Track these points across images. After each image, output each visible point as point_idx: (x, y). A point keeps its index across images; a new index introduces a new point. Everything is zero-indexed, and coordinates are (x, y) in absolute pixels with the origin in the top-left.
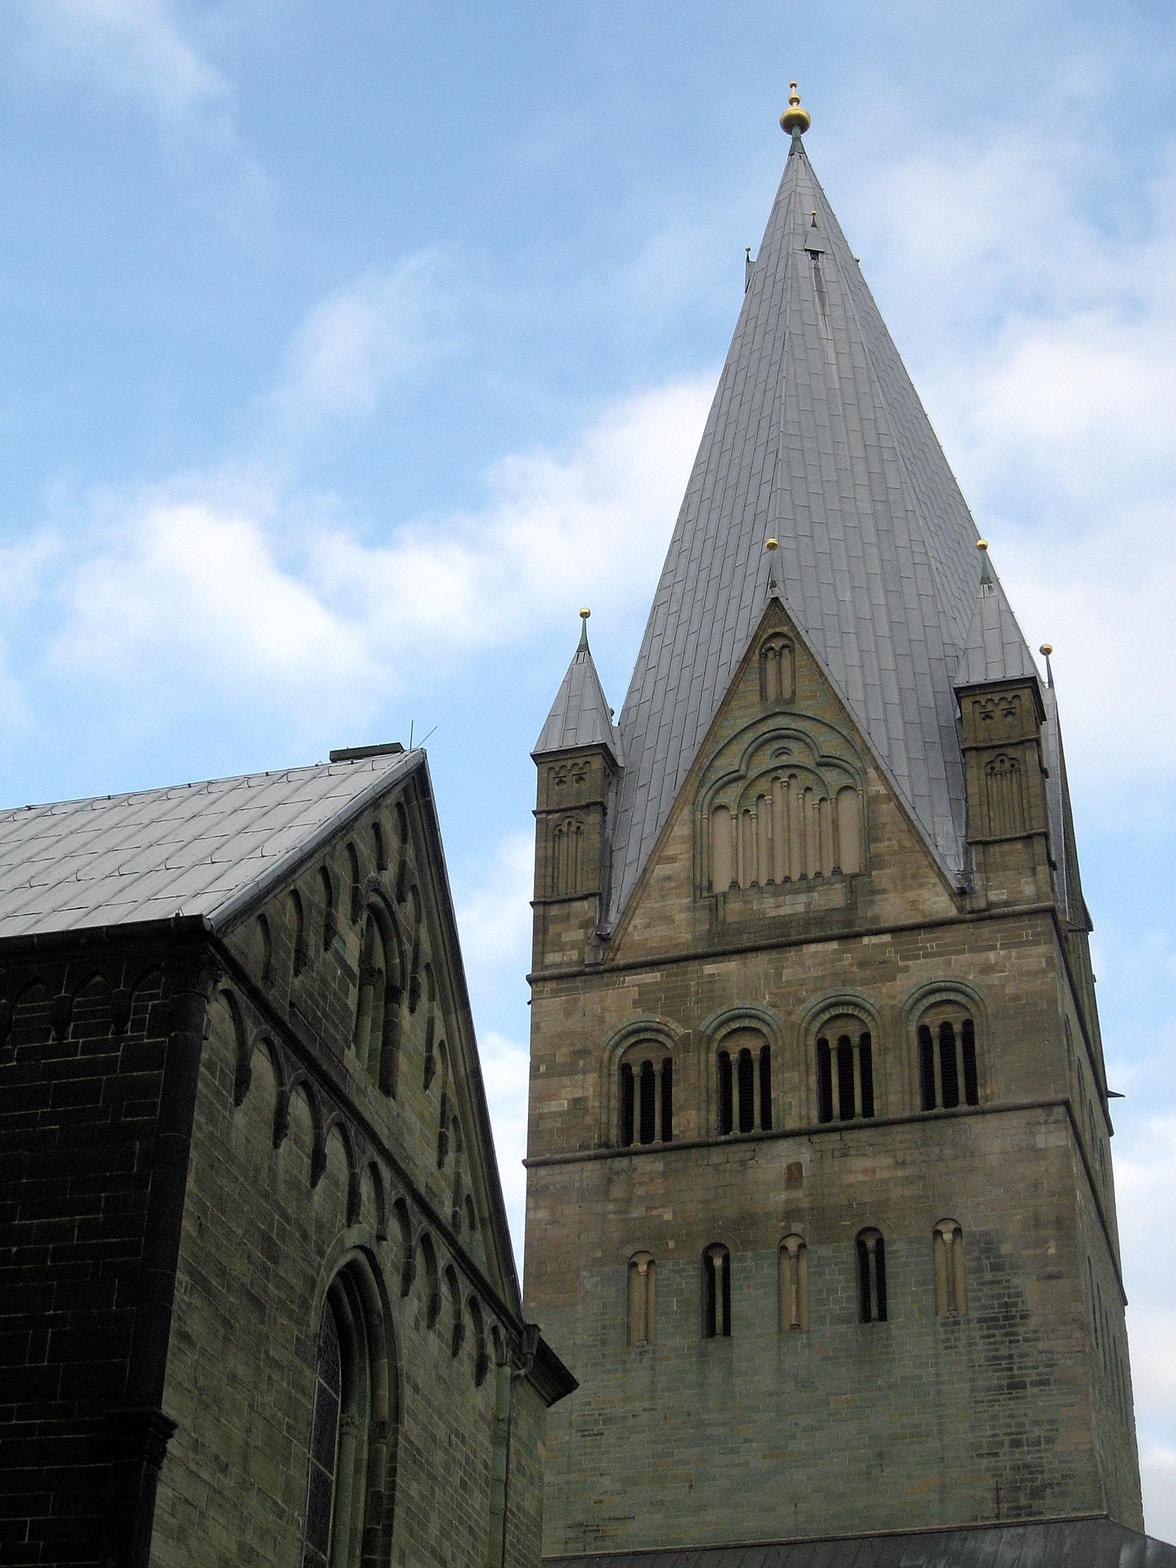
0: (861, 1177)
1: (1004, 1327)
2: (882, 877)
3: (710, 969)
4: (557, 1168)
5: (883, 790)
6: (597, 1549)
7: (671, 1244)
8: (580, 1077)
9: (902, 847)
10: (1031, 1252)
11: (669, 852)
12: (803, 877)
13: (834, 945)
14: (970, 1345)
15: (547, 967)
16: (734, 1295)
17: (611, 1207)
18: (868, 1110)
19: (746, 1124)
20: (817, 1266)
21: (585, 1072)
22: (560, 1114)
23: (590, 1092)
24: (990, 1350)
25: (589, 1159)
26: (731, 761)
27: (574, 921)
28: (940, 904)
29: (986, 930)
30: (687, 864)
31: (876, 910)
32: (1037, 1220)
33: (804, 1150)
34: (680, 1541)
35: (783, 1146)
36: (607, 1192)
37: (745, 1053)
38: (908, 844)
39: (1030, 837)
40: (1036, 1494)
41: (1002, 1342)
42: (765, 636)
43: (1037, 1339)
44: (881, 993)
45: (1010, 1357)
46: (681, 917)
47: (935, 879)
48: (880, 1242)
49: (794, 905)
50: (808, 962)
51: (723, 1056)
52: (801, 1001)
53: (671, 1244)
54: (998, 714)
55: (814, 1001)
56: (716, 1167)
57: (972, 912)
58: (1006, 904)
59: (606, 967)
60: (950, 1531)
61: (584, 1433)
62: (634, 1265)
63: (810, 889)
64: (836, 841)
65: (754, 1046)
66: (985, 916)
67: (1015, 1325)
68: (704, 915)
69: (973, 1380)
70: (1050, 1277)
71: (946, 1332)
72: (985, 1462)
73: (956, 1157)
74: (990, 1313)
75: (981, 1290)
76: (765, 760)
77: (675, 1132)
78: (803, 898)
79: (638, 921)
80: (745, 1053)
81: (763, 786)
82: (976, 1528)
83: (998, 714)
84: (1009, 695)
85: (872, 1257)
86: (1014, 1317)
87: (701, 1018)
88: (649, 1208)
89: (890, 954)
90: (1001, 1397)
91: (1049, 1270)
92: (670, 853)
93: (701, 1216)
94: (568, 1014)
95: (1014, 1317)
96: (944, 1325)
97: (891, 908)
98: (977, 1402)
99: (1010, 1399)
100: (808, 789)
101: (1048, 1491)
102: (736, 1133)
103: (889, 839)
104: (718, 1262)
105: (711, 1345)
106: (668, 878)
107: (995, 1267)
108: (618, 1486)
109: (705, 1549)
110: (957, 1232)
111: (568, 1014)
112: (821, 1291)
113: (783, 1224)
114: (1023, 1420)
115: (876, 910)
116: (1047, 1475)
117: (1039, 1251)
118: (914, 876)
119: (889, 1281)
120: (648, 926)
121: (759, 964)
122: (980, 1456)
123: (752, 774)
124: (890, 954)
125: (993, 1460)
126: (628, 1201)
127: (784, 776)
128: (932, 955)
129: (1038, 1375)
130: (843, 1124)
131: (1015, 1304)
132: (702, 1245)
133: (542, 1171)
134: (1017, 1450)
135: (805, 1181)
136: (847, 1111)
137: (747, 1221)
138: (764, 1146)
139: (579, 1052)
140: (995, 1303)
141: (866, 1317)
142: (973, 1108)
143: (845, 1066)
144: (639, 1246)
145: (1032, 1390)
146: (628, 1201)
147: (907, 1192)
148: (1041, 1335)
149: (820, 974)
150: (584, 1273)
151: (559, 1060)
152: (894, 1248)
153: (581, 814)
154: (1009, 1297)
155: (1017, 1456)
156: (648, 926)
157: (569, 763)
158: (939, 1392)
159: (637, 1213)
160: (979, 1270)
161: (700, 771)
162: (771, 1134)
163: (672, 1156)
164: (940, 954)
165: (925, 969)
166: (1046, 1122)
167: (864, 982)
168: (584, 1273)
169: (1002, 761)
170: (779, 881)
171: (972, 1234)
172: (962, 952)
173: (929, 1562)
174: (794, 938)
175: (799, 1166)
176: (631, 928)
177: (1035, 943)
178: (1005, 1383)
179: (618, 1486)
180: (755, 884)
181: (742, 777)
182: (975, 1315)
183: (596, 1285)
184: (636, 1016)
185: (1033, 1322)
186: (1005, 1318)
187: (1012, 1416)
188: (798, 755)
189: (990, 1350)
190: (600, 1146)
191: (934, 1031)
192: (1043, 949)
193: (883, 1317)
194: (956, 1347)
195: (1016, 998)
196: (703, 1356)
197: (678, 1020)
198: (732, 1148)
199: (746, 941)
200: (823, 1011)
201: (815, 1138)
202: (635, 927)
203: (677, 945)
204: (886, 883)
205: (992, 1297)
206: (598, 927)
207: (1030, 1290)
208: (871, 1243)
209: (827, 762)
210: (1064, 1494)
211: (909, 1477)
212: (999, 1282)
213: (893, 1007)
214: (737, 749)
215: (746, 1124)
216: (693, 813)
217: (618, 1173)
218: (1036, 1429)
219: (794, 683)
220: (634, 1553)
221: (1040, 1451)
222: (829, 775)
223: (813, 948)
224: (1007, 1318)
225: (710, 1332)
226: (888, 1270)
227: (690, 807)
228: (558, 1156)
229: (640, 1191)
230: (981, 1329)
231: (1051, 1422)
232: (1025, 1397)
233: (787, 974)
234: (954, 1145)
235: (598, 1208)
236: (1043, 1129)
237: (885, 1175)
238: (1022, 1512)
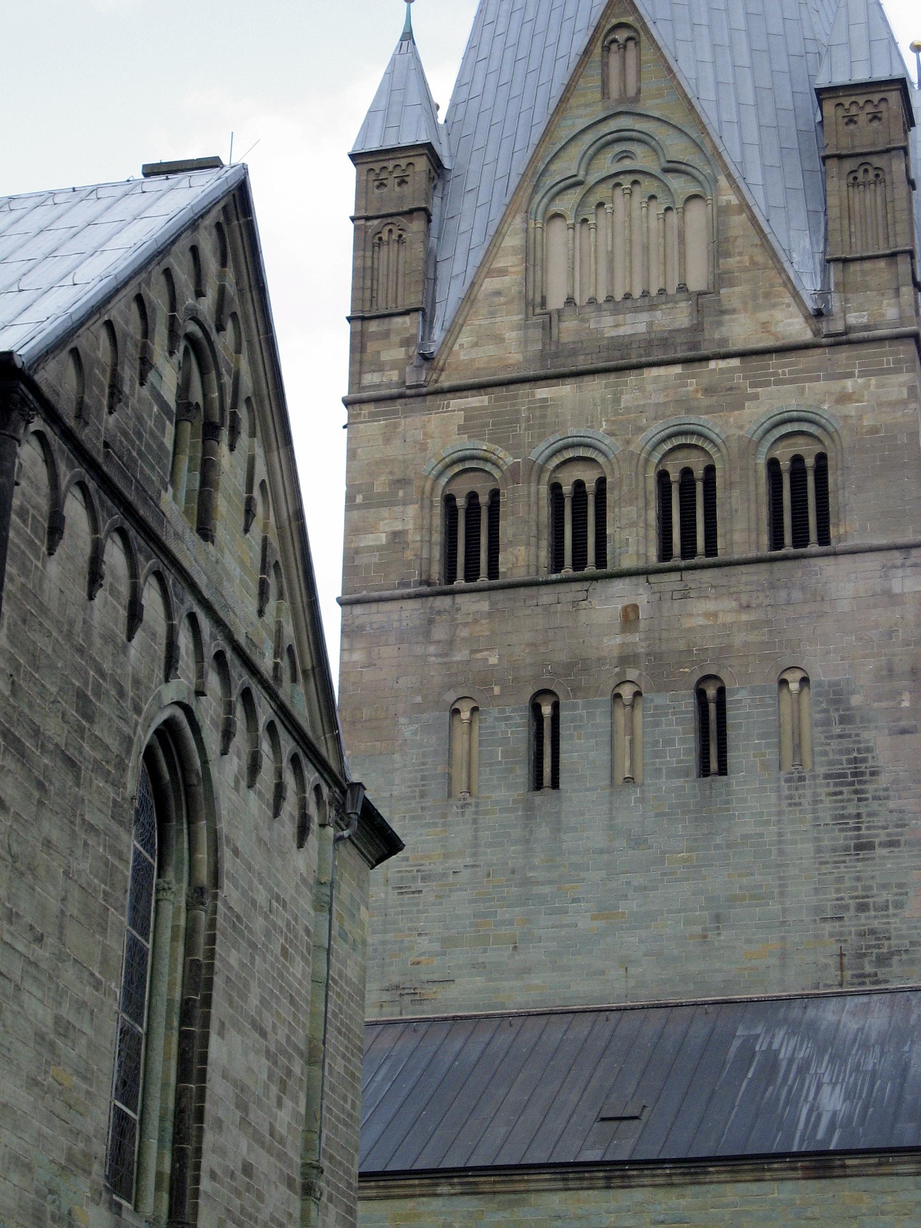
0: (701, 621)
1: (852, 784)
2: (731, 295)
3: (542, 392)
4: (374, 607)
5: (734, 201)
6: (415, 1014)
7: (497, 690)
8: (398, 509)
9: (753, 263)
10: (884, 704)
11: (500, 263)
12: (645, 294)
13: (678, 369)
14: (815, 802)
15: (364, 388)
16: (563, 745)
17: (432, 649)
18: (711, 549)
19: (579, 562)
20: (653, 715)
21: (405, 504)
22: (379, 548)
23: (410, 526)
24: (836, 809)
25: (409, 597)
26: (568, 165)
27: (395, 339)
28: (796, 327)
29: (843, 355)
30: (519, 277)
31: (725, 331)
32: (890, 670)
33: (641, 591)
34: (503, 1006)
35: (619, 586)
36: (427, 634)
37: (579, 485)
38: (760, 259)
39: (894, 255)
40: (882, 961)
41: (849, 800)
42: (608, 27)
43: (887, 798)
44: (727, 422)
45: (858, 816)
46: (511, 336)
47: (788, 299)
48: (721, 691)
49: (635, 325)
50: (649, 387)
51: (556, 488)
52: (641, 429)
53: (497, 690)
54: (863, 118)
55: (656, 429)
56: (547, 608)
57: (827, 336)
58: (866, 328)
59: (430, 388)
60: (789, 999)
61: (401, 890)
62: (456, 712)
63: (652, 307)
64: (683, 256)
65: (589, 477)
66: (842, 340)
67: (865, 782)
68: (536, 334)
70: (903, 732)
71: (789, 788)
72: (828, 927)
73: (805, 602)
75: (829, 744)
76: (606, 165)
77: (502, 569)
78: (644, 317)
79: (465, 339)
80: (579, 485)
81: (604, 192)
82: (817, 996)
83: (863, 118)
84: (876, 98)
85: (712, 707)
86: (862, 774)
87: (532, 446)
88: (474, 652)
89: (739, 379)
90: (847, 858)
91: (903, 723)
92: (501, 265)
93: (528, 661)
94: (387, 441)
95: (862, 774)
96: (788, 780)
97: (741, 330)
98: (822, 863)
99: (858, 860)
100: (652, 197)
101: (896, 958)
102: (568, 571)
103: (740, 254)
104: (547, 710)
105: (538, 798)
106: (498, 293)
107: (843, 720)
108: (436, 947)
109: (529, 1015)
110: (805, 681)
111: (387, 441)
112: (657, 742)
113: (617, 669)
114: (870, 882)
115: (725, 331)
116: (893, 942)
117: (891, 704)
118: (767, 295)
119: (731, 733)
120: (476, 344)
121: (596, 387)
122: (824, 920)
123: (592, 179)
124: (739, 379)
125: (837, 924)
126: (451, 643)
127: (626, 181)
129: (888, 835)
130: (683, 563)
132: (530, 691)
133: (358, 610)
134: (863, 915)
135: (642, 625)
136: (689, 550)
137: (579, 667)
138: (598, 585)
139: (399, 481)
140: (844, 758)
141: (704, 771)
142: (824, 549)
143: (687, 503)
144: (462, 692)
145: (880, 852)
146: (451, 643)
147: (753, 637)
148: (892, 794)
149: (662, 400)
150: (402, 720)
151: (378, 489)
152: (735, 698)
153: (403, 220)
154: (859, 751)
155: (863, 921)
156: (476, 344)
157: (390, 165)
158: (781, 852)
159: (460, 655)
161: (534, 176)
162: (604, 572)
163: (499, 595)
165: (775, 397)
166: (903, 565)
167: (710, 410)
168: (402, 720)
169: (866, 171)
170: (619, 297)
171: (820, 684)
172: (818, 379)
173: (767, 1031)
174: (634, 360)
175: (635, 607)
176: (456, 347)
177: (896, 371)
178: (852, 843)
179: (436, 947)
180: (592, 301)
181: (580, 183)
182: (821, 770)
183: (415, 733)
184: (461, 444)
185: (883, 780)
186: (854, 775)
187: (858, 879)
188: (642, 159)
189: (836, 809)
190: (421, 583)
191: (785, 464)
192: (905, 377)
193: (723, 770)
194: (800, 804)
195: (874, 430)
196: (530, 810)
197: (506, 449)
198: (562, 588)
199: (582, 363)
200: (664, 440)
201: (652, 578)
202: (461, 345)
203: (508, 366)
204: (736, 303)
205: (841, 752)
206: (421, 346)
207: (881, 744)
208: (711, 692)
209: (674, 168)
210: (912, 962)
211: (748, 941)
212: (850, 736)
213: (740, 438)
214: (576, 151)
215: (579, 562)
216: (526, 221)
217: (439, 613)
218: (884, 893)
219: (639, 80)
220: (454, 1018)
221: (887, 916)
222: (677, 183)
223: (655, 372)
224: (855, 775)
225: (538, 784)
226: (729, 721)
227: (523, 214)
228: (375, 594)
229: (464, 633)
230: (828, 785)
231: (900, 886)
232: (874, 858)
233: (627, 399)
234: (803, 588)
235: (419, 650)
236: (900, 572)
237: (729, 618)
238: (867, 980)
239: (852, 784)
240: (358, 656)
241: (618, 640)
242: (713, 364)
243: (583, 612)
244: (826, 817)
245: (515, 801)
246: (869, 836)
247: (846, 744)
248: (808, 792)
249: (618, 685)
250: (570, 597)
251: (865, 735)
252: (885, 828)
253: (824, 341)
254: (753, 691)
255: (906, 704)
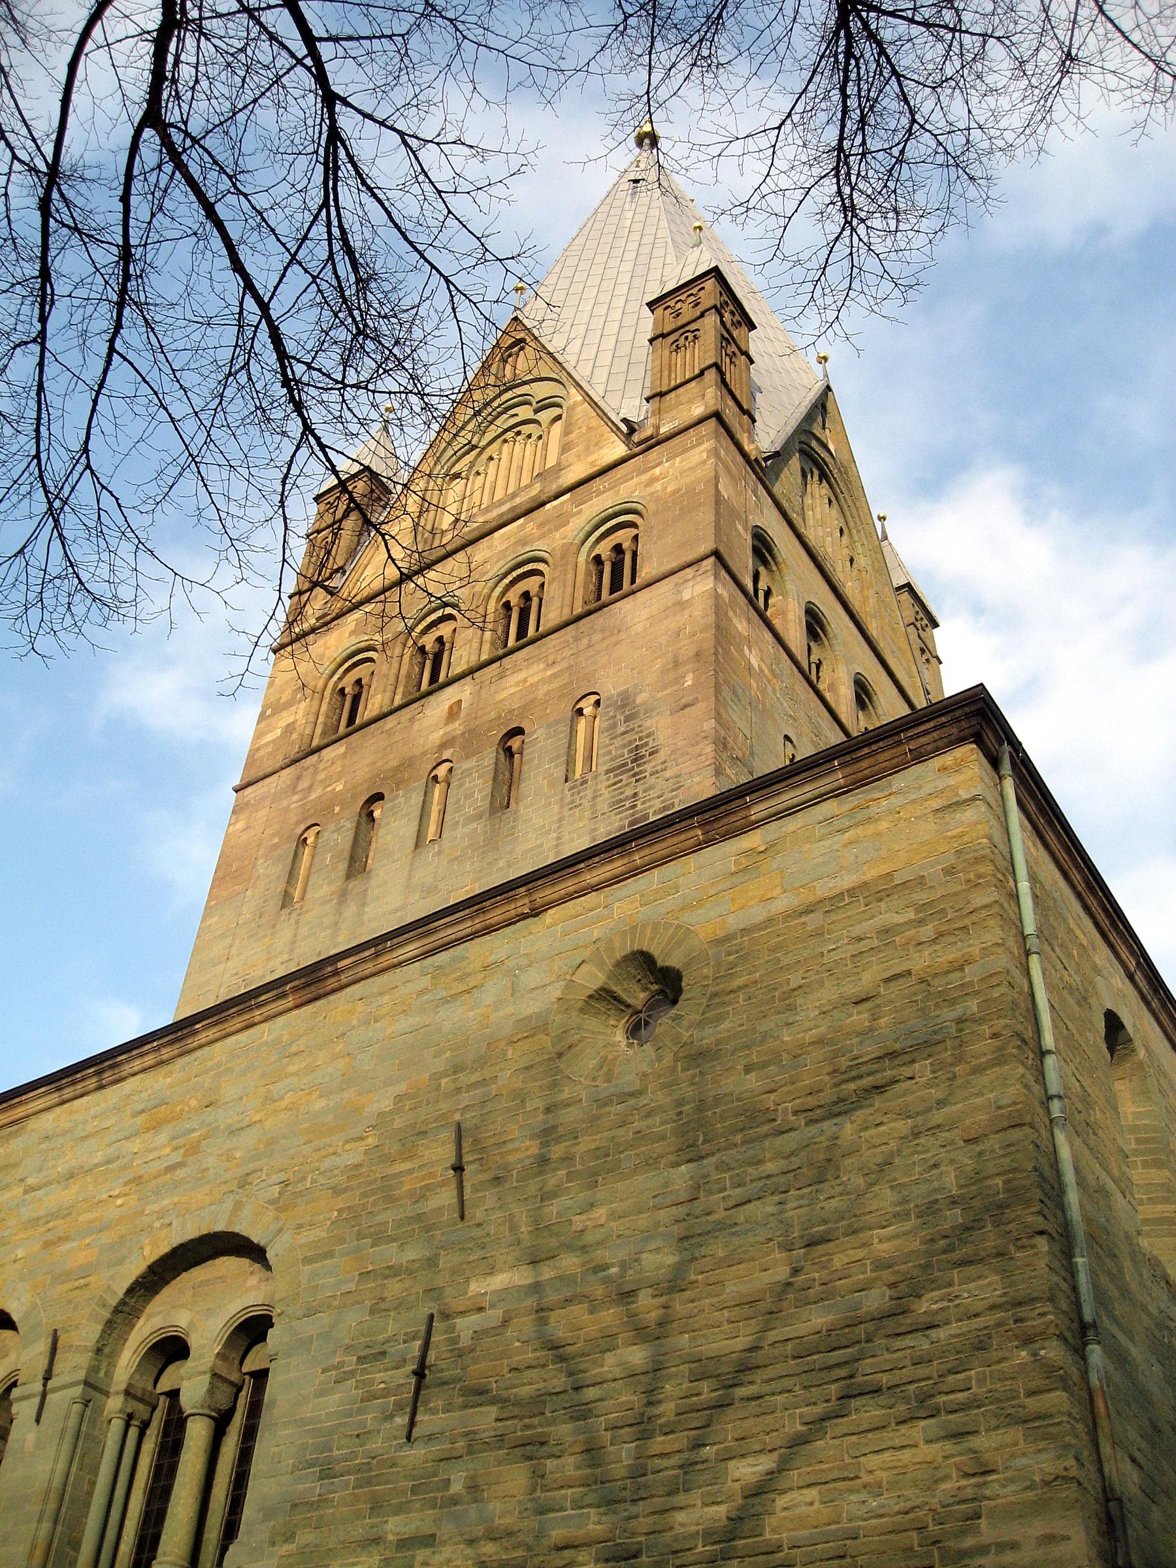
0: (512, 690)
1: (630, 770)
17: (296, 798)
29: (653, 454)
45: (635, 794)
53: (337, 809)
69: (594, 830)
74: (619, 761)
84: (694, 291)
88: (326, 787)
117: (675, 688)
128: (603, 492)
131: (646, 744)
135: (462, 714)
160: (614, 726)
164: (610, 489)
166: (694, 577)
167: (542, 536)
169: (686, 338)
185: (662, 755)
188: (524, 412)
192: (706, 445)
201: (477, 675)
205: (624, 746)
212: (633, 729)
234: (603, 630)
239: (633, 768)
240: (240, 825)
241: (441, 732)
242: (548, 506)
243: (417, 723)
244: (603, 806)
245: (332, 893)
246: (645, 809)
247: (628, 738)
248: (589, 793)
249: (435, 768)
250: (409, 716)
251: (648, 723)
252: (659, 797)
253: (637, 450)
254: (549, 726)
255: (690, 683)
